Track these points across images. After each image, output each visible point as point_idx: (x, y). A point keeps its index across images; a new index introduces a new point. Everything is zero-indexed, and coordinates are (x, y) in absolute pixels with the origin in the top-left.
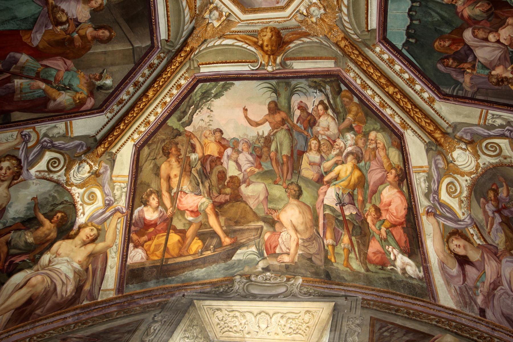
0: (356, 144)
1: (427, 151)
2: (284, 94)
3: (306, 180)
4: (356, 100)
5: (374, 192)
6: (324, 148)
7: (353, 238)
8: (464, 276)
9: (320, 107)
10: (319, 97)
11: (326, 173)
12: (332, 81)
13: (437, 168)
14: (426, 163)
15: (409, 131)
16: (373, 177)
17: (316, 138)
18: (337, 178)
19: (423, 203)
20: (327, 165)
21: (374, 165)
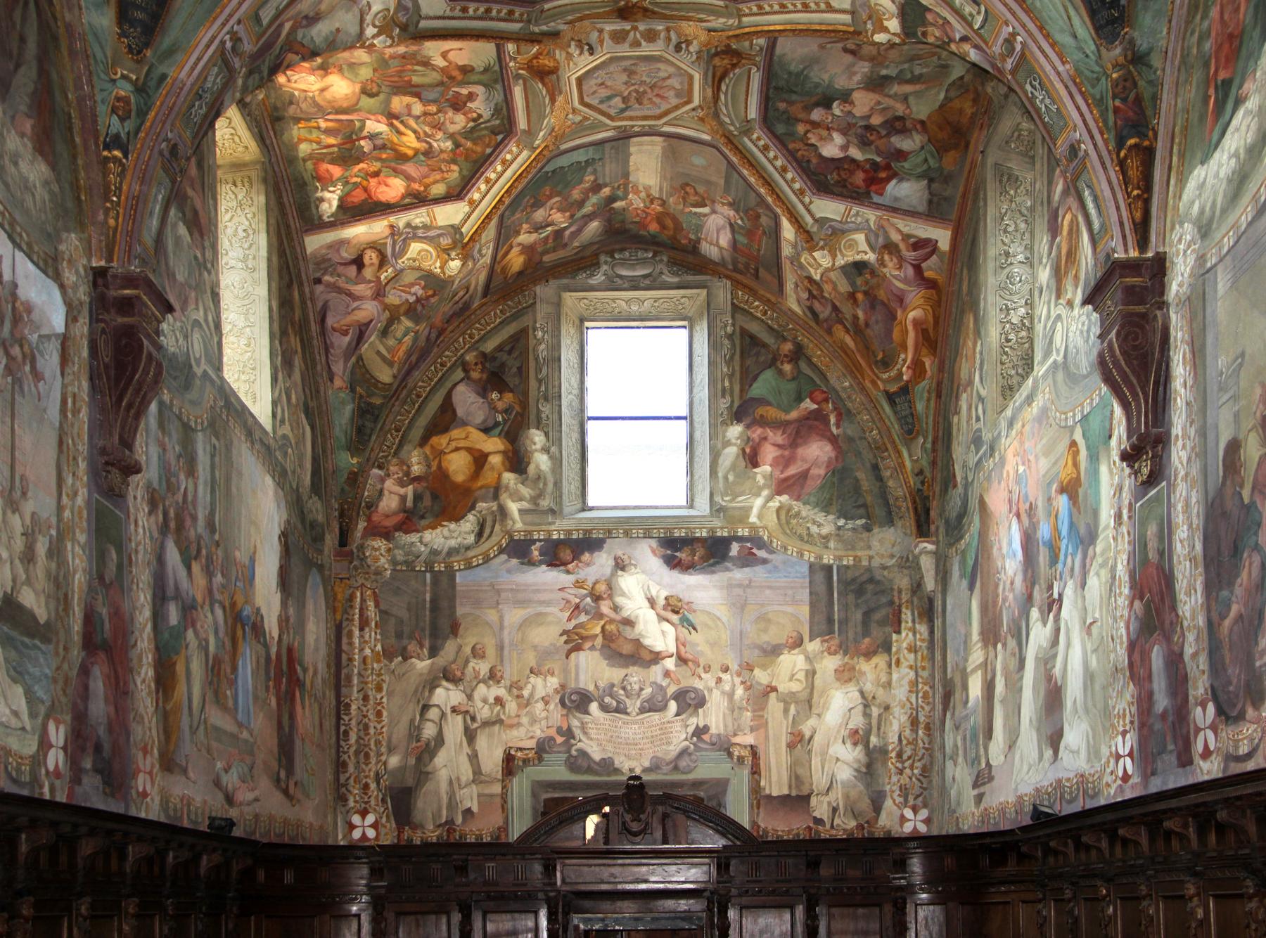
0: (442, 151)
1: (452, 226)
2: (484, 78)
3: (388, 102)
4: (488, 151)
5: (395, 170)
6: (429, 119)
7: (336, 149)
8: (345, 264)
9: (475, 115)
10: (487, 114)
11: (402, 122)
12: (504, 127)
13: (439, 236)
14: (440, 224)
15: (467, 209)
16: (409, 168)
17: (439, 111)
18: (399, 133)
19: (401, 220)
20: (412, 122)
21: (425, 170)
